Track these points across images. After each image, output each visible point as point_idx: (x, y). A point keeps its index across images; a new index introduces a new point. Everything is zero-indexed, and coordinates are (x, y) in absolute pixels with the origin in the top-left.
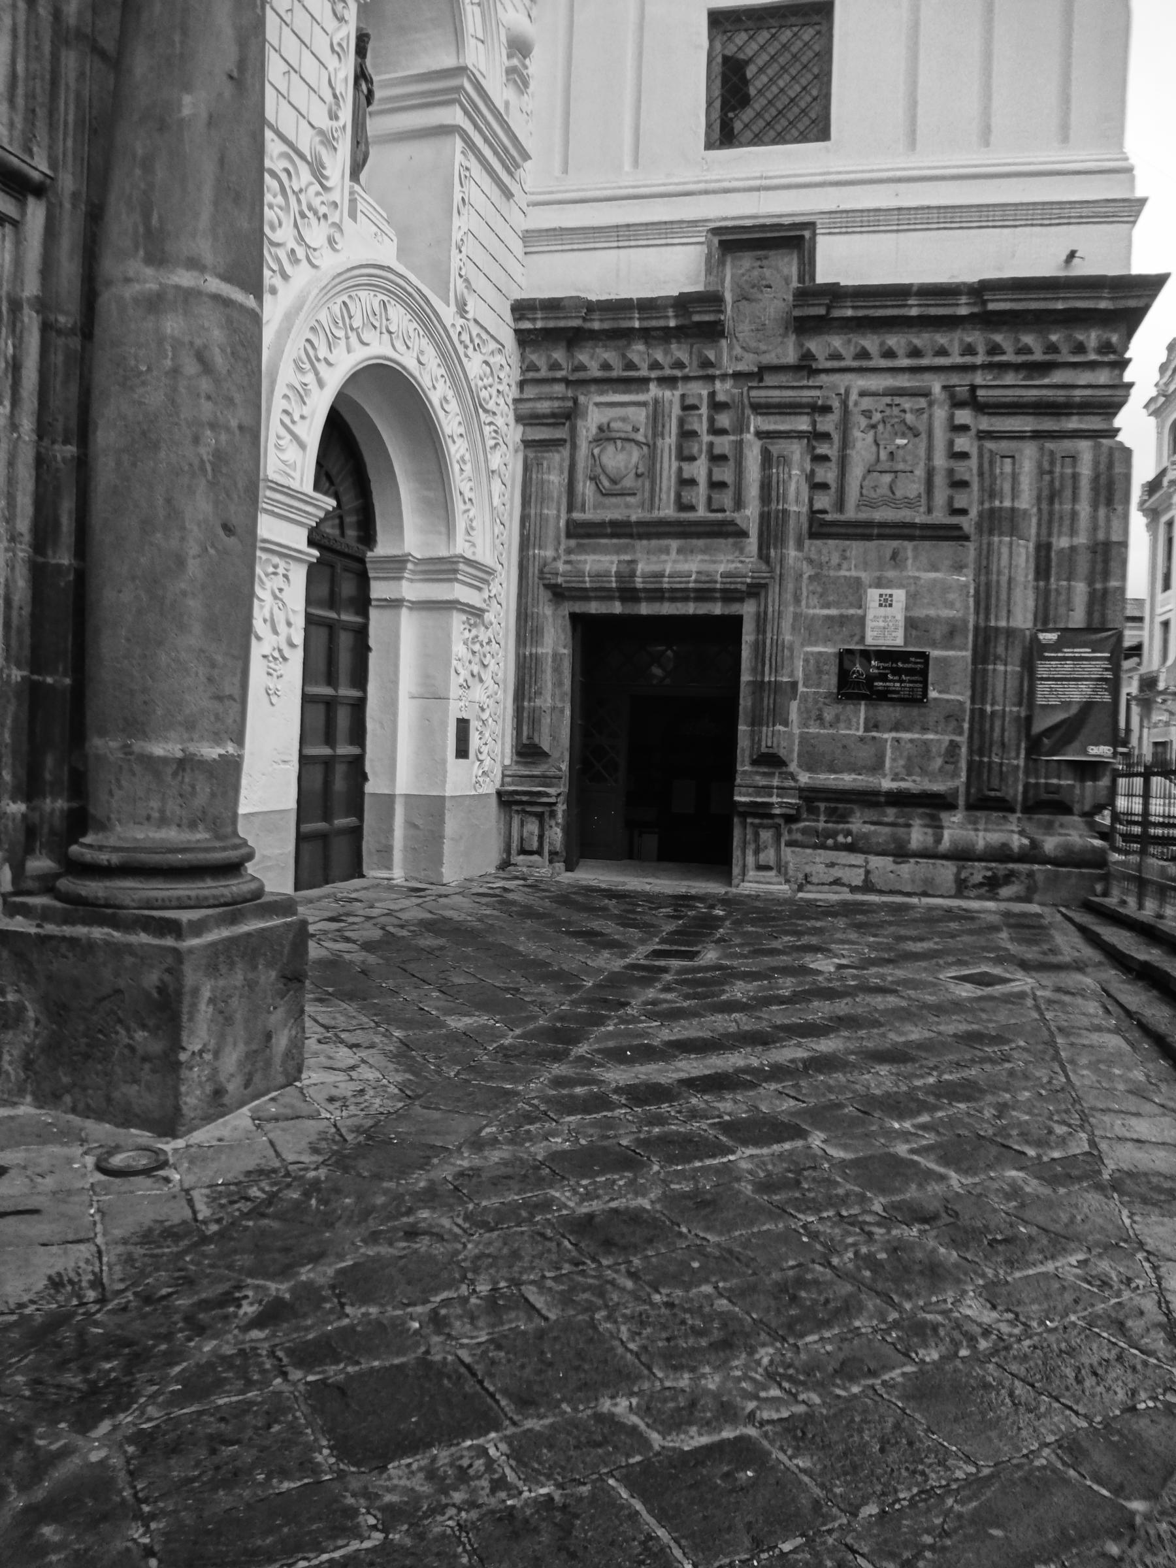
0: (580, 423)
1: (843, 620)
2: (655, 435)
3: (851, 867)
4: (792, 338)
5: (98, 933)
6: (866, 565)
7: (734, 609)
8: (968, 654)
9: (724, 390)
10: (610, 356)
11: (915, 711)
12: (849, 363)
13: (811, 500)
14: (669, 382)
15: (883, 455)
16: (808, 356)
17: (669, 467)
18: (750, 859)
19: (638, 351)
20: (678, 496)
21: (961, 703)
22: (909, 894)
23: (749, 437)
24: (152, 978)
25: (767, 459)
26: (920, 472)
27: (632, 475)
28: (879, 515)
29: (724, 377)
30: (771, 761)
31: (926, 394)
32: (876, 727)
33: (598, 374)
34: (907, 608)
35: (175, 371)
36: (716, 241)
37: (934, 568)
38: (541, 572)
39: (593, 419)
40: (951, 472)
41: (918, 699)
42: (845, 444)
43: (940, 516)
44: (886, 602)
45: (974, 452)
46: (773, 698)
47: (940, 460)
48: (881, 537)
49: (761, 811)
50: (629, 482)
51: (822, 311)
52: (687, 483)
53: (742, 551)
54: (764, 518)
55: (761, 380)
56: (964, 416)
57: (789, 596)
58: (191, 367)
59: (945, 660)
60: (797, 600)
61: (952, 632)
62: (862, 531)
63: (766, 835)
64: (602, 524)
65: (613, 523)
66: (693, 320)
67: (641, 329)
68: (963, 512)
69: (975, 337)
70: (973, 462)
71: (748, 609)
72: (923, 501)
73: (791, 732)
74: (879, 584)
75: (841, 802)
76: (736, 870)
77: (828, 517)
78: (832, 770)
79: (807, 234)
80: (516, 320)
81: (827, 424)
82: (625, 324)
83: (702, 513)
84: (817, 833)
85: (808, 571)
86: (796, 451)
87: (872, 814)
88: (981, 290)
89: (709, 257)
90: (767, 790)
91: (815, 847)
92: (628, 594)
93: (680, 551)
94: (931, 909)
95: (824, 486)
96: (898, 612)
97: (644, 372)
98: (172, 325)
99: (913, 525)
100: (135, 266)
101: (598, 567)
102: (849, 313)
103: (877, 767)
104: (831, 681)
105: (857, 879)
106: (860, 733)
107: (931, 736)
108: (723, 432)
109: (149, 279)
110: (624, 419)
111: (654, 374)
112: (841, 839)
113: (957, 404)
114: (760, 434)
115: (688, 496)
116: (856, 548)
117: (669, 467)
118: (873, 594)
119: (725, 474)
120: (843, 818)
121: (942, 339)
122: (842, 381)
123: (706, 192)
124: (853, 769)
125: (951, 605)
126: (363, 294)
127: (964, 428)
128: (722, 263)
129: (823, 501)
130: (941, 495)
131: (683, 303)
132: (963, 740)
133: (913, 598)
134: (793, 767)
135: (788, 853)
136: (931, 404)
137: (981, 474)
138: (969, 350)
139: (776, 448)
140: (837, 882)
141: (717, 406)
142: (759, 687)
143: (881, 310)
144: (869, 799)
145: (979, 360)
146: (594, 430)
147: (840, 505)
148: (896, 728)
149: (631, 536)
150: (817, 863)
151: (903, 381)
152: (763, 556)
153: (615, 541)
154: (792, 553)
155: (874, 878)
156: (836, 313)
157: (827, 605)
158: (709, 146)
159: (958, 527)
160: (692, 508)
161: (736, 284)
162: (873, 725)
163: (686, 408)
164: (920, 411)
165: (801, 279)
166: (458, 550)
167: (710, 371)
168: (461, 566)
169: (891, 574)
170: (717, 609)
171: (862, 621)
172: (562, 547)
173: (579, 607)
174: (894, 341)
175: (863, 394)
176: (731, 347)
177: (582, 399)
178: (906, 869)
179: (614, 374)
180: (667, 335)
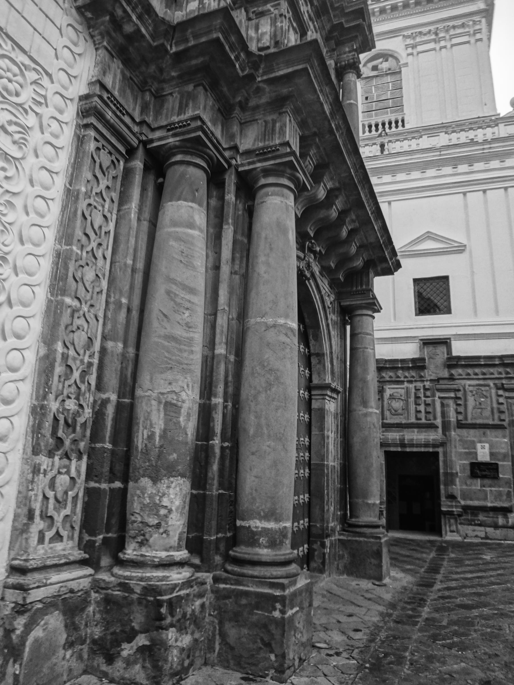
0: (384, 394)
1: (469, 453)
2: (407, 397)
3: (481, 531)
4: (446, 370)
5: (362, 539)
6: (475, 437)
7: (436, 450)
8: (510, 463)
9: (428, 384)
10: (391, 374)
11: (496, 481)
12: (464, 377)
13: (457, 417)
14: (410, 382)
15: (478, 403)
16: (452, 375)
17: (412, 407)
18: (448, 529)
19: (400, 373)
20: (416, 416)
21: (510, 479)
22: (501, 540)
23: (437, 398)
24: (375, 548)
25: (443, 405)
26: (489, 408)
28: (479, 421)
29: (427, 381)
30: (452, 497)
31: (488, 386)
32: (484, 486)
33: (388, 379)
34: (490, 449)
35: (370, 428)
36: (422, 342)
37: (496, 437)
40: (498, 409)
41: (496, 477)
42: (466, 400)
43: (497, 422)
44: (483, 448)
45: (505, 403)
46: (451, 477)
47: (495, 405)
48: (480, 428)
49: (450, 513)
50: (400, 411)
51: (455, 363)
52: (418, 412)
53: (437, 432)
54: (444, 423)
55: (438, 382)
56: (501, 392)
57: (453, 446)
58: (372, 427)
59: (503, 465)
60: (455, 447)
61: (505, 457)
62: (473, 426)
63: (452, 521)
64: (394, 424)
65: (397, 424)
66: (418, 365)
68: (504, 420)
69: (501, 370)
70: (505, 406)
71: (440, 450)
72: (491, 417)
73: (457, 488)
74: (480, 442)
75: (475, 510)
76: (443, 532)
77: (463, 422)
78: (471, 499)
79: (448, 341)
81: (460, 394)
82: (396, 366)
83: (423, 421)
84: (468, 520)
85: (458, 438)
86: (451, 402)
87: (486, 514)
88: (501, 357)
89: (420, 347)
90: (452, 506)
91: (469, 525)
92: (402, 444)
93: (418, 432)
94: (509, 544)
95: (460, 413)
96: (487, 450)
97: (402, 379)
98: (369, 419)
99: (489, 425)
100: (361, 408)
101: (392, 437)
102: (463, 363)
103: (486, 499)
104: (468, 472)
105: (483, 535)
106: (479, 488)
107: (501, 489)
108: (428, 397)
109: (364, 410)
110: (397, 393)
111: (406, 380)
112: (476, 522)
113: (498, 388)
114: (439, 398)
115: (419, 416)
116: (472, 431)
117: (412, 407)
118: (479, 445)
119: (430, 409)
120: (476, 515)
121: (491, 370)
122: (463, 382)
123: (417, 328)
124: (478, 499)
125: (503, 448)
127: (501, 396)
128: (424, 348)
129: (460, 417)
130: (496, 416)
131: (413, 360)
132: (512, 490)
133: (491, 447)
134: (459, 499)
135: (459, 527)
136: (490, 389)
137: (508, 409)
138: (500, 373)
139: (445, 402)
140: (476, 536)
141: (425, 389)
142: (446, 474)
143: (472, 362)
144: (484, 509)
145: (504, 376)
147: (466, 418)
148: (490, 486)
149: (402, 427)
150: (469, 530)
151: (481, 382)
152: (444, 433)
154: (453, 433)
155: (488, 535)
156: (459, 363)
157: (465, 448)
158: (416, 315)
159: (503, 425)
160: (421, 419)
161: (428, 353)
162: (483, 486)
163: (416, 390)
164: (487, 391)
165: (448, 354)
167: (423, 379)
169: (483, 439)
170: (431, 450)
171: (476, 453)
173: (387, 449)
174: (477, 370)
175: (469, 386)
176: (428, 372)
177: (384, 387)
178: (498, 532)
179: (393, 379)
180: (408, 368)
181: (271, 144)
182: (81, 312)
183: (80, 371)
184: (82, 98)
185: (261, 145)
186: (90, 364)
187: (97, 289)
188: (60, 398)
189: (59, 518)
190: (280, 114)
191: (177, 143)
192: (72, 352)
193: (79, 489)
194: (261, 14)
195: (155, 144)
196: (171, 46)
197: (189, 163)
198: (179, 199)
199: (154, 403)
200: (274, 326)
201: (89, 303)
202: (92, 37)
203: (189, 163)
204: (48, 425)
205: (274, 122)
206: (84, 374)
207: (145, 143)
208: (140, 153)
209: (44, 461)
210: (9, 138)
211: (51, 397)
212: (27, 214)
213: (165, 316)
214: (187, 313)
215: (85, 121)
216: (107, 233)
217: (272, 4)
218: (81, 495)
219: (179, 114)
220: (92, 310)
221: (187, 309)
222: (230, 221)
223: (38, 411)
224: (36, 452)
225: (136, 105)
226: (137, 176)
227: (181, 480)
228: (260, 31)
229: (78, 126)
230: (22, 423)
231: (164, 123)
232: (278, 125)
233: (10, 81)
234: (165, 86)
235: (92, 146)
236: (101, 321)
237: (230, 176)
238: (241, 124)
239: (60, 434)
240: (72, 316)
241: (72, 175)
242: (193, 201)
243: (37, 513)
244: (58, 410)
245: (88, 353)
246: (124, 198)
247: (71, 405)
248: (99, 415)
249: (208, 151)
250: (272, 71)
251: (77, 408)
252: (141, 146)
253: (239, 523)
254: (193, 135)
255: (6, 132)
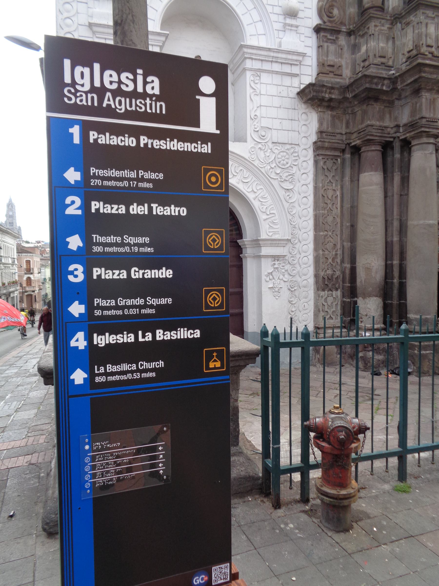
181: (415, 119)
182: (329, 236)
183: (331, 258)
184: (315, 143)
185: (410, 119)
186: (336, 255)
187: (335, 223)
188: (324, 270)
189: (330, 312)
190: (419, 97)
191: (361, 143)
192: (326, 252)
193: (338, 301)
194: (408, 24)
195: (353, 144)
196: (349, 94)
197: (368, 151)
198: (365, 172)
199: (361, 268)
200: (417, 225)
201: (332, 231)
202: (314, 108)
203: (368, 151)
204: (321, 280)
205: (416, 104)
206: (333, 260)
207: (349, 144)
208: (348, 150)
209: (322, 293)
210: (288, 182)
211: (320, 270)
212: (300, 206)
213: (362, 231)
214: (372, 228)
215: (317, 153)
216: (336, 197)
217: (413, 15)
218: (339, 303)
219: (362, 124)
220: (334, 232)
221: (372, 226)
222: (397, 170)
223: (316, 276)
224: (318, 290)
225: (343, 124)
226: (347, 163)
227: (375, 298)
228: (407, 39)
229: (315, 156)
230: (311, 280)
231: (356, 130)
232: (418, 105)
233: (283, 160)
234: (354, 108)
235: (321, 163)
236: (339, 236)
237: (396, 144)
238: (401, 106)
239: (326, 283)
240: (325, 238)
241: (316, 179)
242: (371, 171)
243: (321, 310)
244: (324, 275)
245: (334, 250)
246: (343, 177)
247: (330, 272)
248: (343, 273)
249: (376, 141)
250: (404, 81)
251: (332, 272)
252: (347, 146)
253: (408, 315)
254: (366, 139)
255: (286, 181)
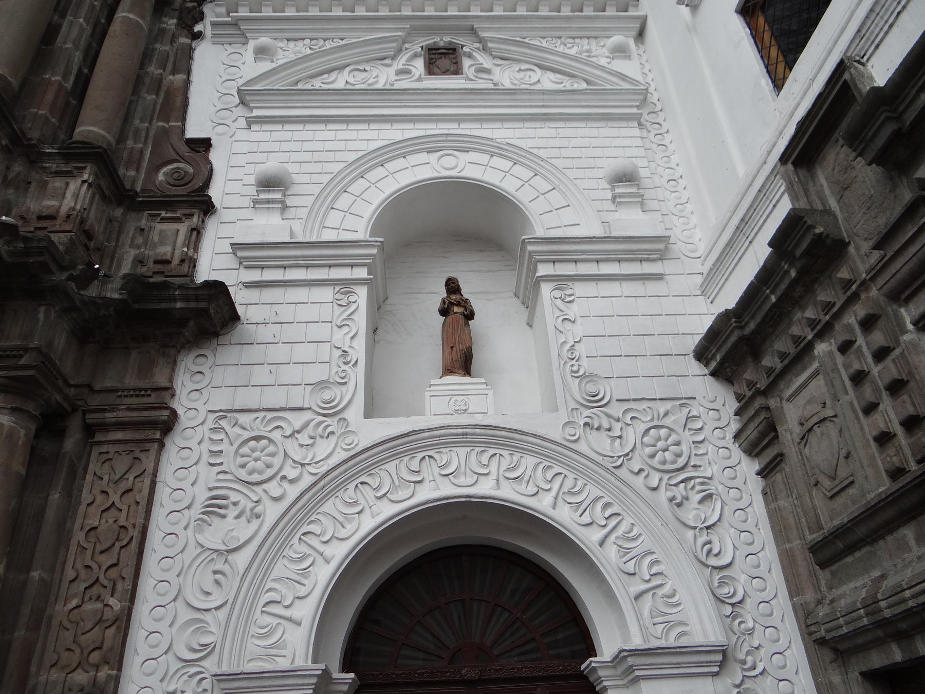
27: (842, 460)
38: (807, 626)
39: (791, 415)
50: (842, 473)
67: (779, 300)
80: (706, 365)
126: (391, 466)
146: (797, 430)
153: (857, 554)
166: (637, 642)
168: (630, 661)
172: (823, 582)
176: (857, 249)
177: (772, 403)
